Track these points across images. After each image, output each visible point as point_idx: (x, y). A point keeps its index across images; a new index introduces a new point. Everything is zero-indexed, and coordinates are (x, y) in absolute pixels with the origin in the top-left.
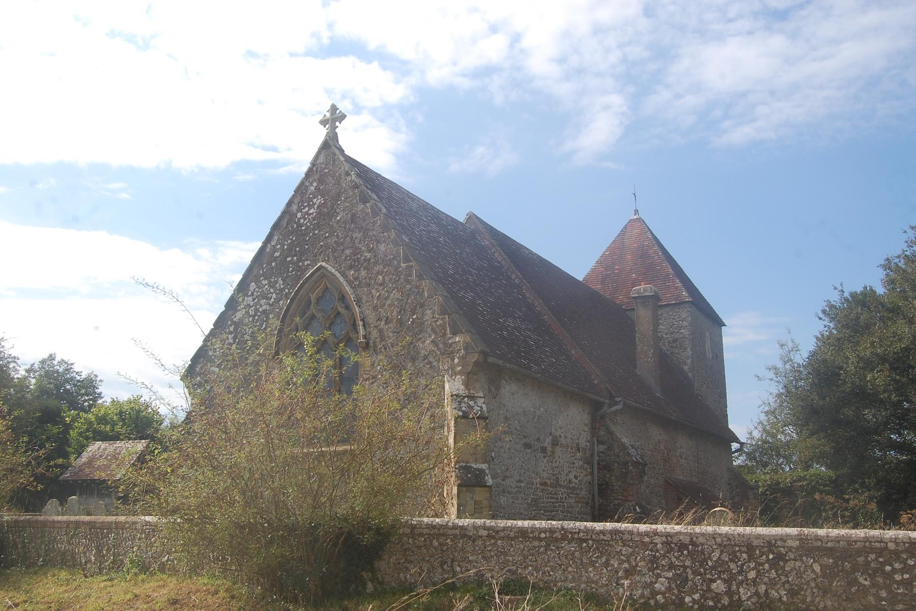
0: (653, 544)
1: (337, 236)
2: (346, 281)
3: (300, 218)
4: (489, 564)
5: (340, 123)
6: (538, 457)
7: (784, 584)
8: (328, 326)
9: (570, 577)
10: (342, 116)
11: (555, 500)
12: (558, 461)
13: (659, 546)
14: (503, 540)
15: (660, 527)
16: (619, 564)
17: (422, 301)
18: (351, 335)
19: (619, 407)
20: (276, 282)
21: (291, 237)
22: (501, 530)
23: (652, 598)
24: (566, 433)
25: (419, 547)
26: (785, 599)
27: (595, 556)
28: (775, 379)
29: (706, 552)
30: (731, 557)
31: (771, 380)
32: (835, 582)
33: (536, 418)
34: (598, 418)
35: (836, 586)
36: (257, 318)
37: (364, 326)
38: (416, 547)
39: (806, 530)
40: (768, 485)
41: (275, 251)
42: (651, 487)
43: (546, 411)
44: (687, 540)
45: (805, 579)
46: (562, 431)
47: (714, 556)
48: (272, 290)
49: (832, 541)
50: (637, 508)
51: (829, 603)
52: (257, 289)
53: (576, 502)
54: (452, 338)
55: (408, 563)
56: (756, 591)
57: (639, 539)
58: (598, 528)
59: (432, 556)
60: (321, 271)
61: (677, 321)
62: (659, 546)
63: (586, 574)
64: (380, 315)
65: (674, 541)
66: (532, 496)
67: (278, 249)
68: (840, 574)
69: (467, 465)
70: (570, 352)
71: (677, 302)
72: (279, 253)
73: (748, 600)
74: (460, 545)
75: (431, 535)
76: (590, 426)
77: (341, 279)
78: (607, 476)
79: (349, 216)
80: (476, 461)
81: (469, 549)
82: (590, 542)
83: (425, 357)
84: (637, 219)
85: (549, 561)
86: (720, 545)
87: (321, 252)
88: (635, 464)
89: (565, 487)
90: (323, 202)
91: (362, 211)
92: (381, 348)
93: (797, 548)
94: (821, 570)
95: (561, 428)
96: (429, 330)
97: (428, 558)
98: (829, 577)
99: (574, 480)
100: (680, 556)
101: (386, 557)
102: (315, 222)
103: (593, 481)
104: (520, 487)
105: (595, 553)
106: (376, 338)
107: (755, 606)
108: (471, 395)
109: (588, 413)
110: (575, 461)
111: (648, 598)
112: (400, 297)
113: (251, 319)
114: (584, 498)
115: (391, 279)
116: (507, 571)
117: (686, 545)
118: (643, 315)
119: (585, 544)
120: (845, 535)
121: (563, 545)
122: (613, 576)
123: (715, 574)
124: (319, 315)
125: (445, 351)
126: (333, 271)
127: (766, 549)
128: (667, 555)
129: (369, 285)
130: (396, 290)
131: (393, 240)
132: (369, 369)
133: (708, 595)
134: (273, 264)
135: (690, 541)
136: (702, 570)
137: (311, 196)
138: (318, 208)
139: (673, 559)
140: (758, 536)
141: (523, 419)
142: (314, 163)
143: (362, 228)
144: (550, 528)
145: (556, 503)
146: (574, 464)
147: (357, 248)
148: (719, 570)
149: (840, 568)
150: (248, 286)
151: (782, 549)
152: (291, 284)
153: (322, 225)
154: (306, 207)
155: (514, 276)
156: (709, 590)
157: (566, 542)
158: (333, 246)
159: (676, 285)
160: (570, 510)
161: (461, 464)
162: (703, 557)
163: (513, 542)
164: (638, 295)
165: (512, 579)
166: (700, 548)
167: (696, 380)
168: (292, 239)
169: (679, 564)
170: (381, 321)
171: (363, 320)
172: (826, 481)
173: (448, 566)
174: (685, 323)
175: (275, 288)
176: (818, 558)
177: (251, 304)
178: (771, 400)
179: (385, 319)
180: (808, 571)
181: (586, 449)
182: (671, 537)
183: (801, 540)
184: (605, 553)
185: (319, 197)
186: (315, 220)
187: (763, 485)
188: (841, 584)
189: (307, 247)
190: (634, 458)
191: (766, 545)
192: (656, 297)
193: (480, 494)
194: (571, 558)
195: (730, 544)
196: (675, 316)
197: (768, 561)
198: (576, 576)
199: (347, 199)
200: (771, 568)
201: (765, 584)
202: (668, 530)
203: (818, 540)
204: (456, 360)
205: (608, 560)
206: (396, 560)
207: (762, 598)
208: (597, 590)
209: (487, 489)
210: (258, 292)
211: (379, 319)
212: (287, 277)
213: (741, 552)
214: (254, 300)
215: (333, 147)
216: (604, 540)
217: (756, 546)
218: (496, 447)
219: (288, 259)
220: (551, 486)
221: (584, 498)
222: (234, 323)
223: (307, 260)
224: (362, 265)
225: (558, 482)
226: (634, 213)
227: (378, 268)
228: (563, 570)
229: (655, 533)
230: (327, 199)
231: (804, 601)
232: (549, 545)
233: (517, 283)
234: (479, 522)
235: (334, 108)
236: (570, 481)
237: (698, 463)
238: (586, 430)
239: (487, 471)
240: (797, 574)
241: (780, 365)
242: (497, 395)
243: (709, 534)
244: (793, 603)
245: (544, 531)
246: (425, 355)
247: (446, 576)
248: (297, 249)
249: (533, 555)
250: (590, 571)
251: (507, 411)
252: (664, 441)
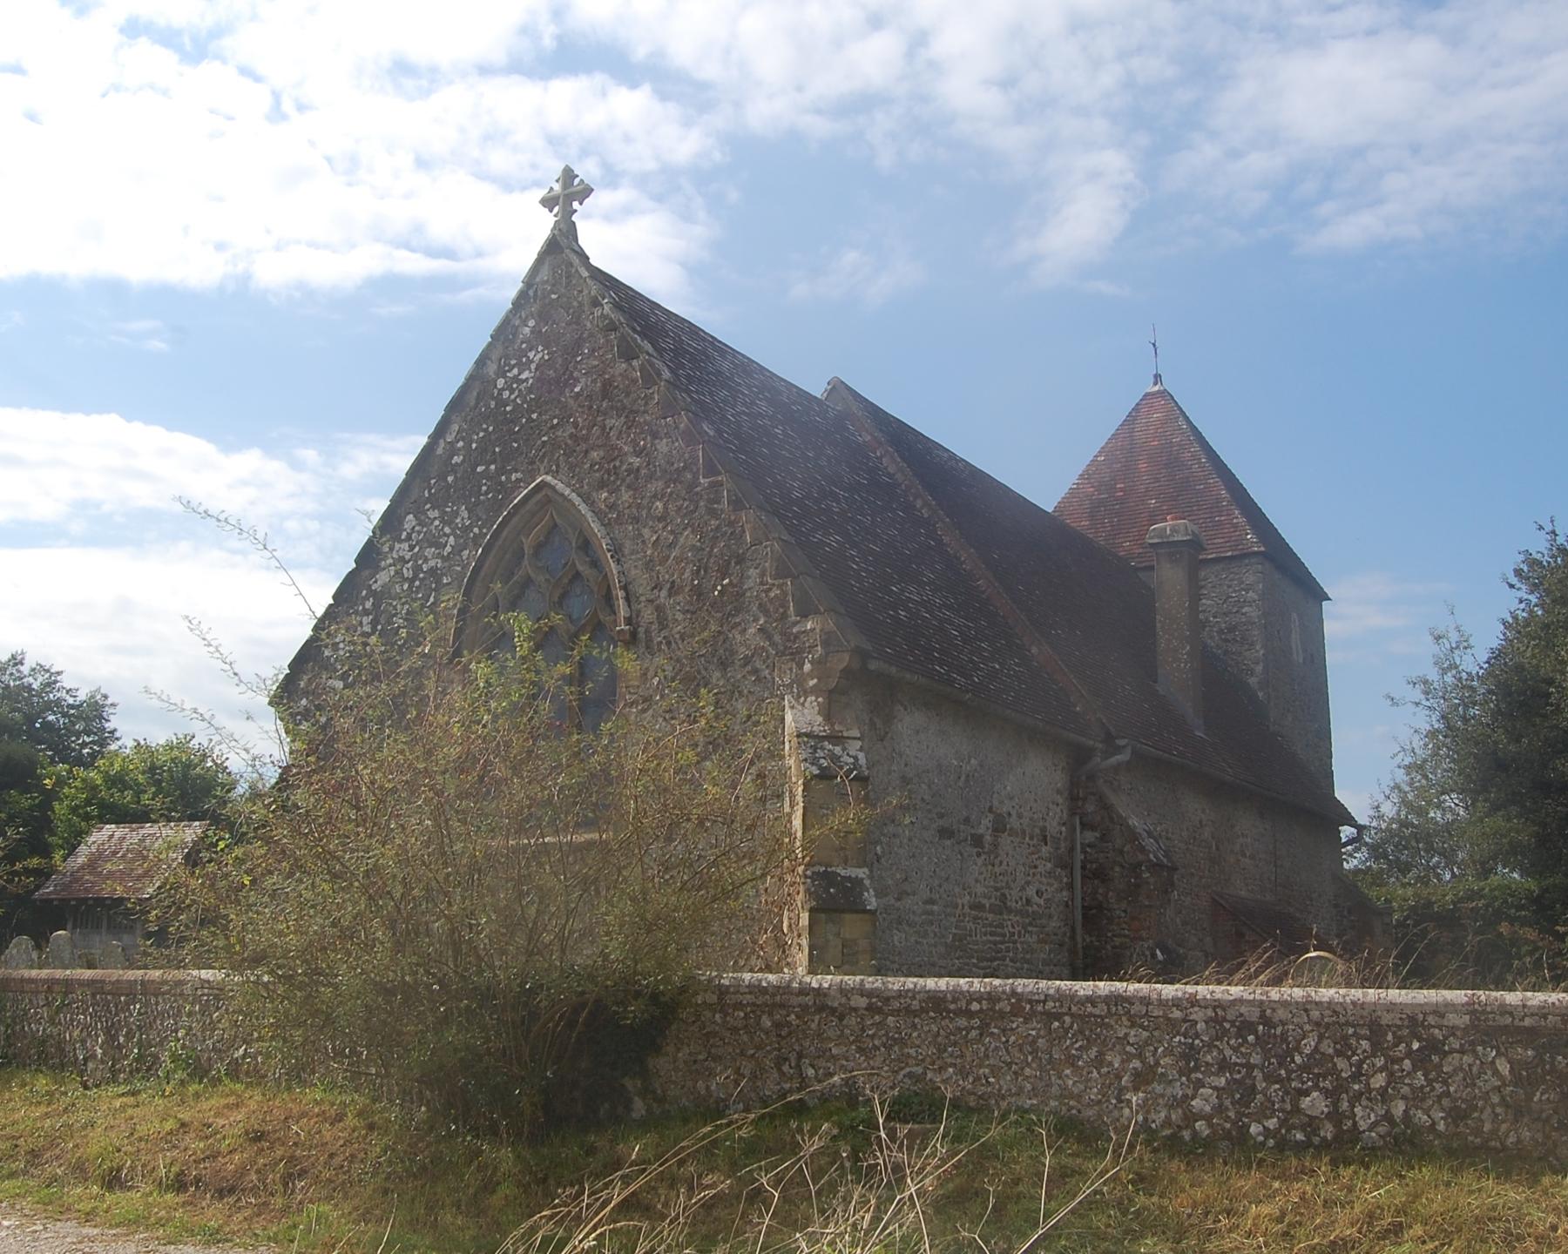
0: (1188, 1024)
1: (576, 425)
2: (593, 512)
3: (503, 389)
4: (871, 1062)
5: (581, 204)
6: (965, 854)
7: (1440, 1097)
8: (556, 599)
9: (1029, 1087)
10: (584, 189)
11: (998, 939)
12: (1005, 863)
13: (1201, 1026)
14: (899, 1015)
15: (1203, 991)
16: (1123, 1061)
17: (741, 551)
18: (601, 617)
19: (1123, 757)
20: (456, 514)
21: (485, 426)
22: (893, 997)
23: (1187, 1127)
25: (735, 1030)
26: (1441, 1126)
27: (1077, 1046)
28: (1424, 702)
29: (1290, 1038)
30: (1338, 1046)
31: (1417, 704)
32: (1538, 1094)
33: (963, 778)
34: (1084, 778)
35: (1540, 1100)
36: (417, 583)
37: (627, 599)
38: (729, 1029)
39: (1482, 995)
40: (1411, 908)
41: (453, 451)
42: (1184, 912)
43: (981, 766)
44: (1253, 1014)
45: (1480, 1088)
47: (1305, 1045)
48: (447, 530)
49: (1532, 1015)
50: (1158, 952)
51: (1526, 1134)
52: (417, 528)
53: (1040, 941)
54: (798, 622)
55: (714, 1060)
56: (1386, 1112)
57: (1161, 1013)
58: (1082, 993)
59: (758, 1048)
60: (544, 493)
61: (1235, 591)
62: (1201, 1026)
63: (1060, 1082)
64: (658, 577)
65: (1229, 1017)
66: (954, 931)
67: (459, 449)
68: (1548, 1078)
69: (829, 869)
70: (1029, 651)
71: (1235, 553)
72: (461, 457)
73: (1370, 1129)
74: (813, 1026)
75: (758, 1006)
76: (1066, 794)
77: (583, 508)
78: (1100, 891)
79: (599, 384)
80: (846, 862)
81: (831, 1033)
82: (1067, 1019)
83: (747, 660)
84: (1158, 392)
85: (987, 1056)
86: (1318, 1024)
87: (544, 456)
88: (1156, 867)
89: (1018, 912)
90: (546, 357)
91: (624, 375)
92: (661, 642)
93: (1466, 1030)
94: (1512, 1068)
96: (754, 609)
97: (752, 1052)
98: (1526, 1084)
99: (1036, 899)
100: (1241, 1045)
101: (670, 1049)
102: (533, 396)
103: (1072, 901)
104: (931, 913)
105: (1076, 1042)
106: (651, 623)
107: (1385, 1141)
108: (836, 734)
109: (1063, 768)
110: (1038, 862)
111: (1178, 1126)
112: (698, 544)
113: (406, 586)
115: (680, 509)
116: (904, 1076)
117: (1252, 1023)
118: (1170, 577)
119: (1057, 1024)
120: (1557, 1003)
121: (1014, 1026)
122: (1111, 1084)
123: (1309, 1079)
124: (540, 578)
125: (786, 648)
126: (567, 492)
127: (1406, 1032)
128: (1216, 1043)
129: (636, 520)
130: (690, 529)
131: (683, 432)
132: (636, 683)
133: (1295, 1121)
134: (450, 479)
135: (1261, 1017)
136: (1283, 1072)
137: (524, 346)
138: (536, 369)
139: (1228, 1052)
140: (1391, 1007)
142: (530, 280)
143: (624, 408)
144: (989, 993)
146: (1036, 867)
147: (614, 447)
148: (1316, 1071)
149: (1548, 1067)
150: (401, 521)
151: (1437, 1031)
152: (484, 517)
153: (546, 403)
154: (514, 366)
155: (919, 503)
156: (1296, 1110)
157: (1021, 1020)
158: (566, 444)
159: (1235, 521)
160: (1028, 956)
161: (816, 869)
162: (1284, 1046)
163: (916, 1020)
165: (915, 1091)
166: (1279, 1030)
168: (486, 430)
169: (1238, 1061)
170: (661, 589)
171: (625, 588)
173: (791, 1067)
174: (1251, 594)
175: (453, 526)
176: (1506, 1049)
177: (407, 557)
178: (1417, 743)
179: (668, 585)
180: (1486, 1074)
181: (1059, 839)
182: (1224, 1010)
183: (1473, 1013)
184: (1096, 1040)
185: (540, 348)
186: (532, 393)
187: (1401, 907)
188: (1548, 1099)
189: (516, 445)
190: (1151, 856)
191: (1406, 1023)
192: (1195, 545)
193: (852, 927)
194: (1030, 1050)
195: (1338, 1022)
196: (1231, 580)
197: (1409, 1053)
198: (1040, 1085)
199: (594, 351)
200: (1415, 1068)
201: (1404, 1098)
202: (1218, 996)
203: (1507, 1012)
204: (807, 667)
205: (1101, 1054)
206: (690, 1054)
207: (1398, 1125)
208: (1079, 1111)
209: (867, 917)
210: (419, 533)
211: (657, 586)
212: (477, 504)
213: (1359, 1037)
214: (412, 548)
215: (567, 251)
216: (1095, 1016)
217: (1388, 1025)
218: (884, 835)
219: (479, 469)
221: (1055, 934)
222: (373, 593)
223: (516, 472)
224: (623, 480)
225: (1005, 904)
226: (1152, 380)
227: (655, 486)
228: (1015, 1073)
229: (1193, 1001)
230: (555, 352)
231: (1478, 1132)
232: (988, 1025)
233: (926, 516)
234: (851, 980)
235: (568, 175)
236: (1028, 902)
237: (1276, 866)
238: (1060, 801)
239: (867, 882)
240: (1465, 1079)
241: (1433, 675)
242: (887, 733)
243: (1297, 1003)
244: (1458, 1134)
245: (979, 997)
246: (746, 657)
247: (787, 1086)
248: (497, 450)
249: (955, 1044)
250: (1067, 1076)
251: (906, 765)
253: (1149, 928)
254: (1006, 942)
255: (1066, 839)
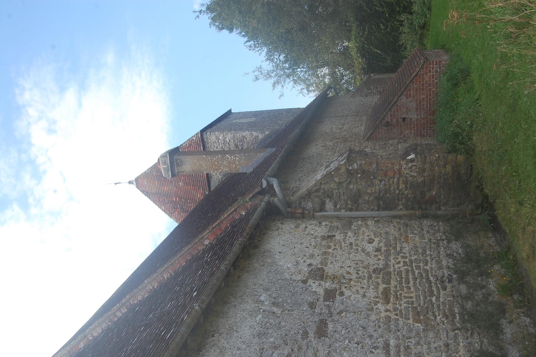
6: (342, 307)
11: (411, 276)
12: (348, 269)
19: (275, 183)
24: (306, 256)
31: (283, 86)
34: (289, 210)
46: (302, 261)
50: (409, 158)
53: (407, 240)
70: (207, 245)
71: (202, 145)
76: (299, 222)
78: (367, 198)
84: (136, 182)
88: (350, 160)
89: (387, 258)
95: (298, 263)
99: (375, 244)
103: (374, 217)
104: (398, 346)
110: (348, 242)
114: (400, 229)
141: (272, 340)
145: (413, 273)
159: (188, 145)
160: (420, 251)
164: (170, 171)
167: (271, 128)
172: (360, 29)
174: (220, 138)
178: (299, 87)
181: (331, 226)
190: (342, 163)
220: (389, 283)
221: (400, 229)
233: (126, 310)
236: (378, 250)
238: (304, 226)
241: (272, 81)
252: (324, 142)
253: (393, 164)
254: (412, 270)
255: (331, 222)
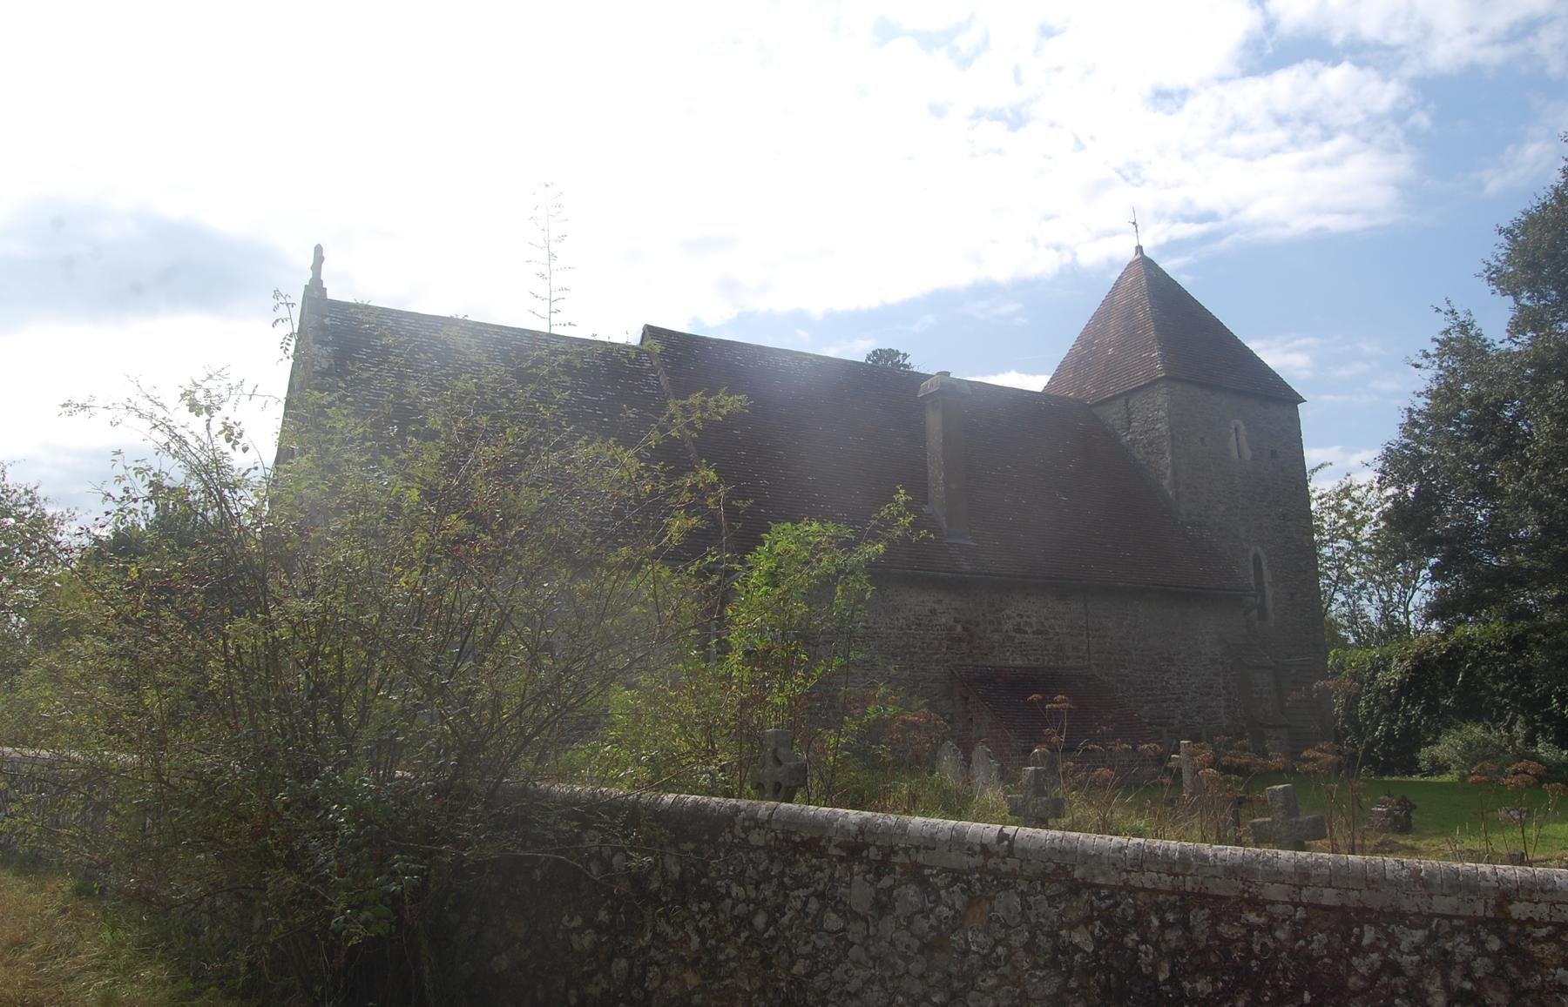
174: (1161, 413)
